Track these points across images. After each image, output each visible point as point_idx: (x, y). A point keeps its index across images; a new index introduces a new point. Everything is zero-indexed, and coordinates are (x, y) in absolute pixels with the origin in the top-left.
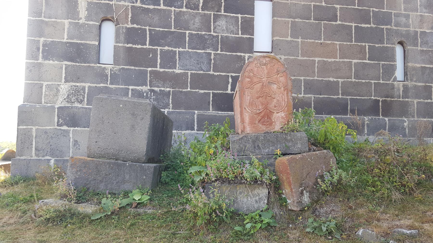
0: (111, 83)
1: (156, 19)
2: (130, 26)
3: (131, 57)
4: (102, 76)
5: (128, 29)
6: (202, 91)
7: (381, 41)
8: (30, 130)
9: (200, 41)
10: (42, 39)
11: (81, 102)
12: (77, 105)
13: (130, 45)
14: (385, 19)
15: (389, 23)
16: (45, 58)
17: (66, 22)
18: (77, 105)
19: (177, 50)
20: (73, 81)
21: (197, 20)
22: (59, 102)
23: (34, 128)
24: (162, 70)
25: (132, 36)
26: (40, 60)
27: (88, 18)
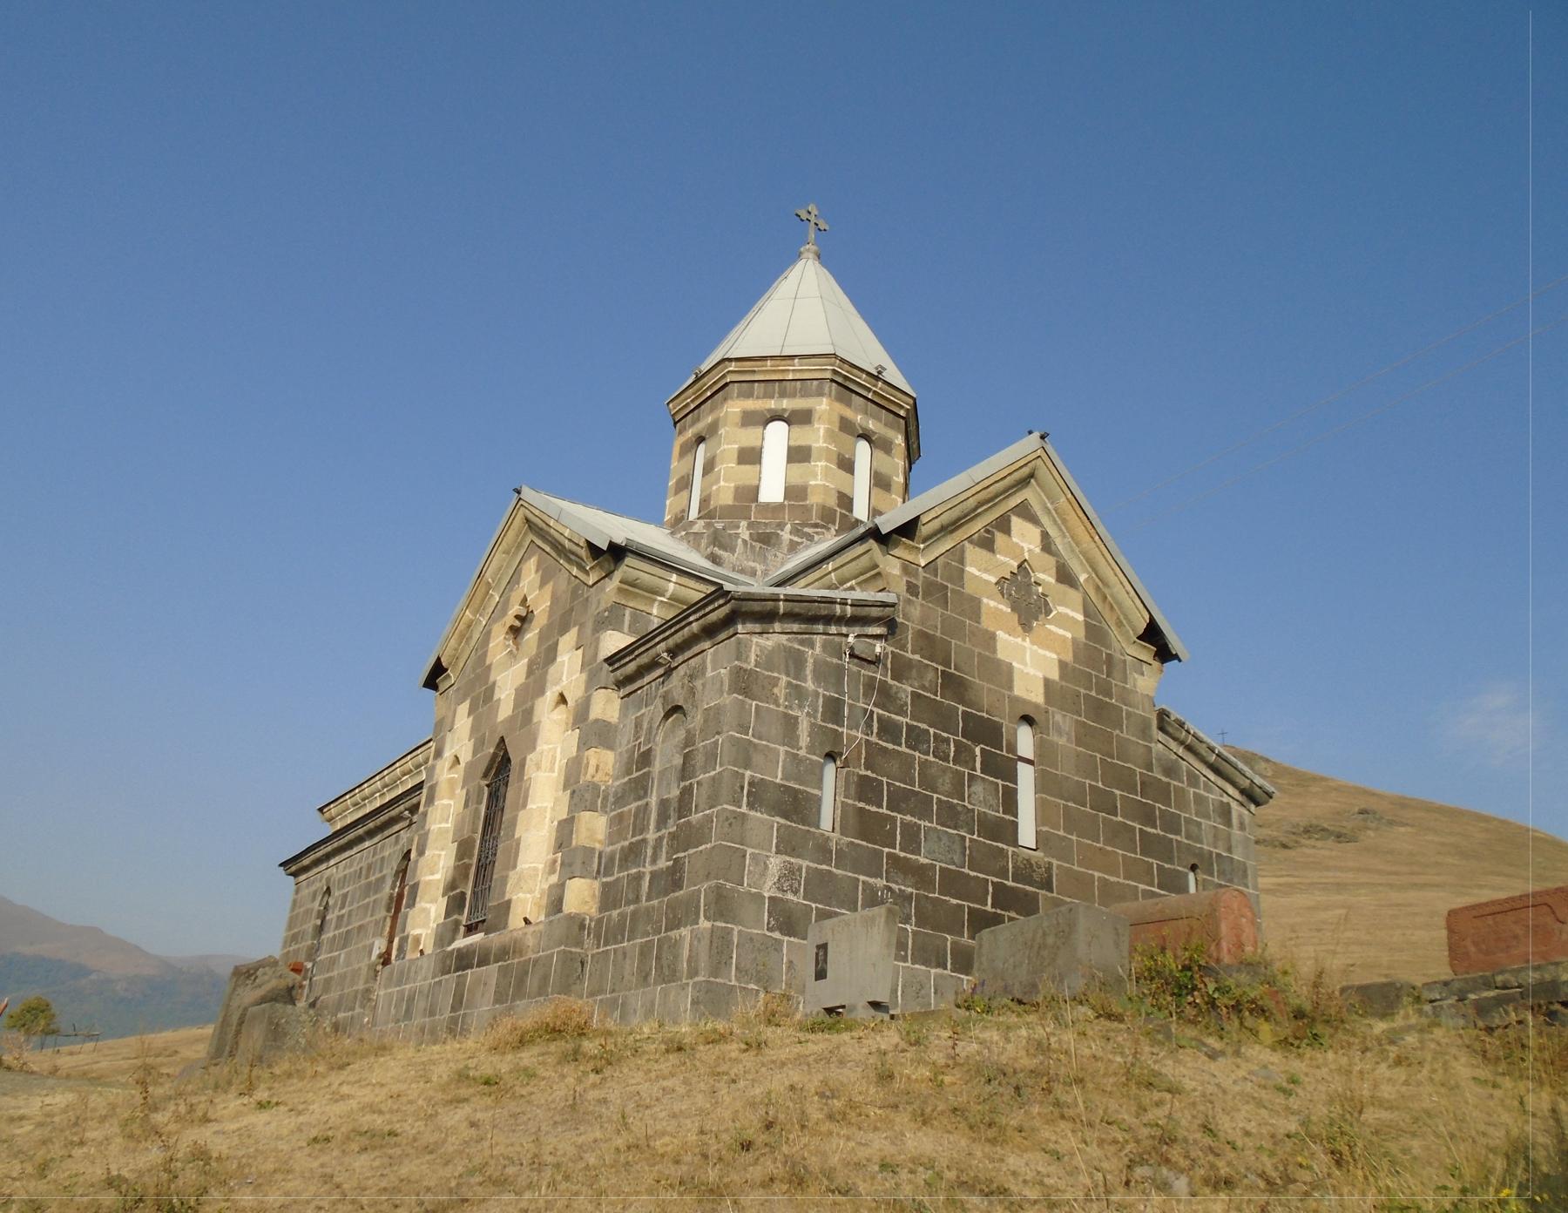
0: (837, 867)
1: (894, 766)
2: (863, 772)
3: (865, 825)
4: (823, 850)
5: (862, 777)
6: (954, 901)
7: (1170, 860)
8: (730, 932)
9: (950, 815)
10: (748, 773)
11: (795, 892)
12: (790, 896)
13: (862, 805)
14: (1172, 824)
15: (1178, 832)
16: (751, 806)
17: (782, 749)
18: (790, 896)
19: (922, 823)
20: (786, 853)
21: (948, 778)
22: (767, 886)
23: (736, 929)
24: (902, 854)
25: (866, 789)
26: (744, 809)
27: (811, 749)
